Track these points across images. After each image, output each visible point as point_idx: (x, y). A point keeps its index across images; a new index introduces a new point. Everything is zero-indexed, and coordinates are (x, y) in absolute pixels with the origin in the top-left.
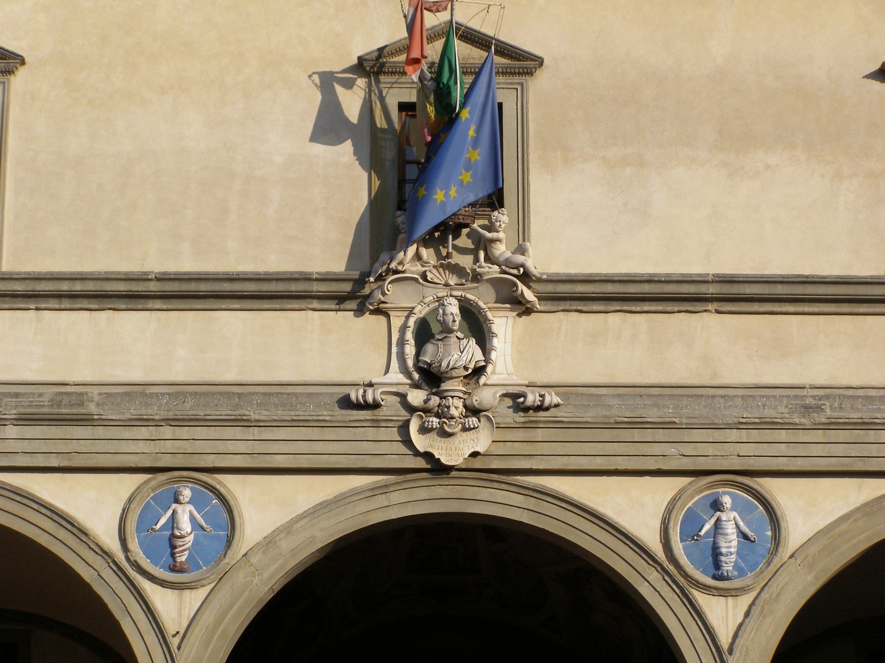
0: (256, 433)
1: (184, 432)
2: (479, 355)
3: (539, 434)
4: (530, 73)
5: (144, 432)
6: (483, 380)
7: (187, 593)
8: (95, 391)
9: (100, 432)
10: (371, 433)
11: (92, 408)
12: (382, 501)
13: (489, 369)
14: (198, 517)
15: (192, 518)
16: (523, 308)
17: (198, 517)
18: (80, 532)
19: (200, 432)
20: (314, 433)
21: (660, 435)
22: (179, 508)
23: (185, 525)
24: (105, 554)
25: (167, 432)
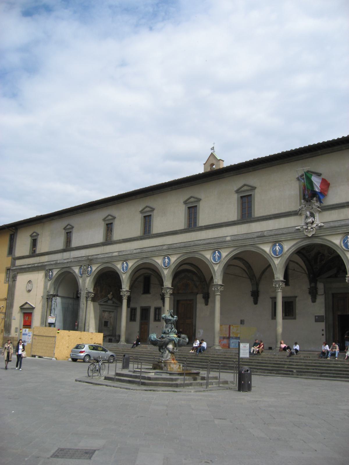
0: (285, 235)
1: (276, 236)
2: (313, 220)
3: (322, 230)
4: (154, 210)
5: (271, 237)
6: (314, 223)
7: (278, 259)
8: (266, 232)
9: (267, 237)
10: (300, 233)
11: (265, 234)
12: (302, 243)
13: (315, 221)
14: (280, 248)
15: (279, 248)
16: (320, 212)
17: (280, 248)
18: (265, 252)
19: (278, 236)
20: (292, 234)
21: (339, 228)
22: (277, 247)
23: (277, 249)
24: (268, 254)
25: (274, 236)
